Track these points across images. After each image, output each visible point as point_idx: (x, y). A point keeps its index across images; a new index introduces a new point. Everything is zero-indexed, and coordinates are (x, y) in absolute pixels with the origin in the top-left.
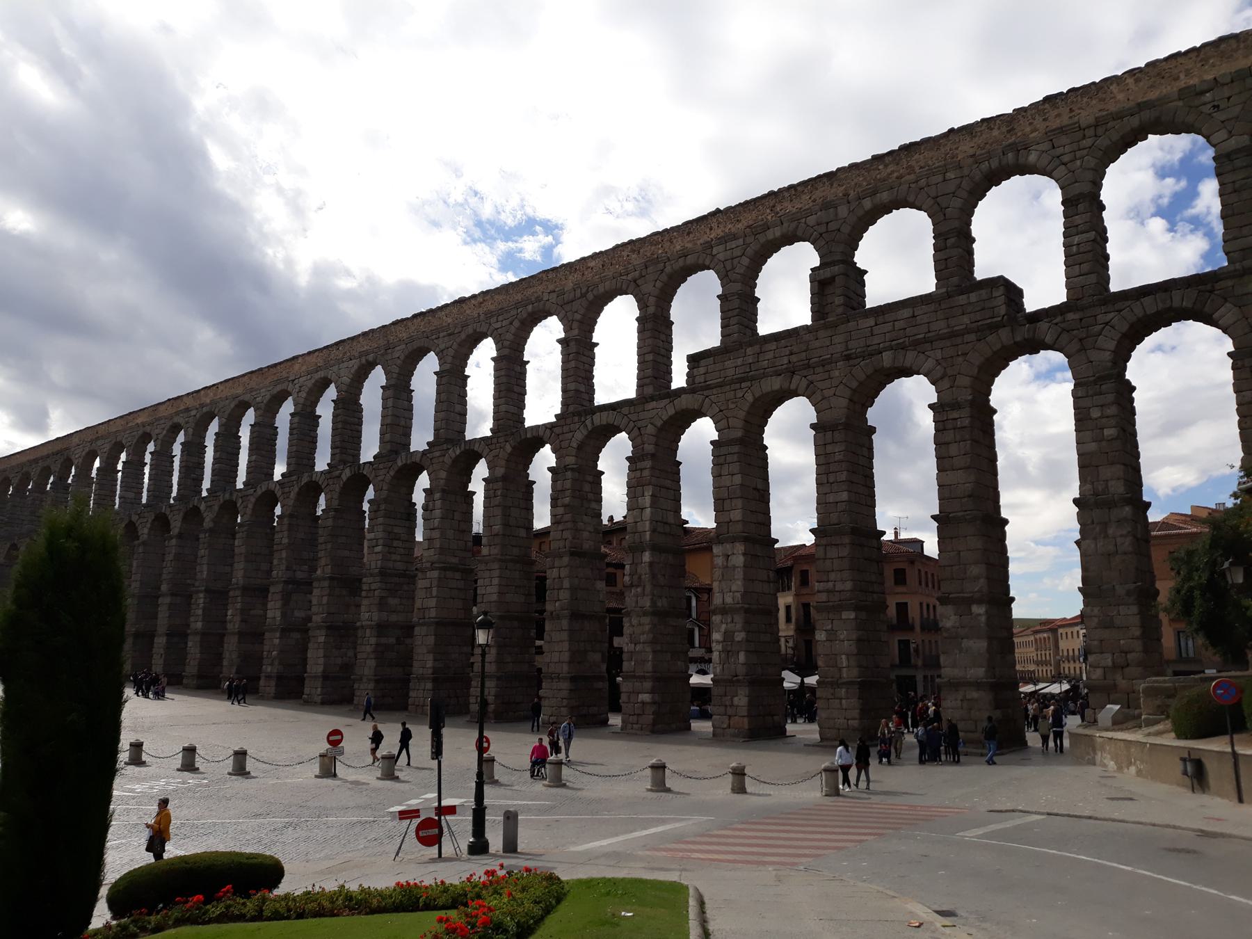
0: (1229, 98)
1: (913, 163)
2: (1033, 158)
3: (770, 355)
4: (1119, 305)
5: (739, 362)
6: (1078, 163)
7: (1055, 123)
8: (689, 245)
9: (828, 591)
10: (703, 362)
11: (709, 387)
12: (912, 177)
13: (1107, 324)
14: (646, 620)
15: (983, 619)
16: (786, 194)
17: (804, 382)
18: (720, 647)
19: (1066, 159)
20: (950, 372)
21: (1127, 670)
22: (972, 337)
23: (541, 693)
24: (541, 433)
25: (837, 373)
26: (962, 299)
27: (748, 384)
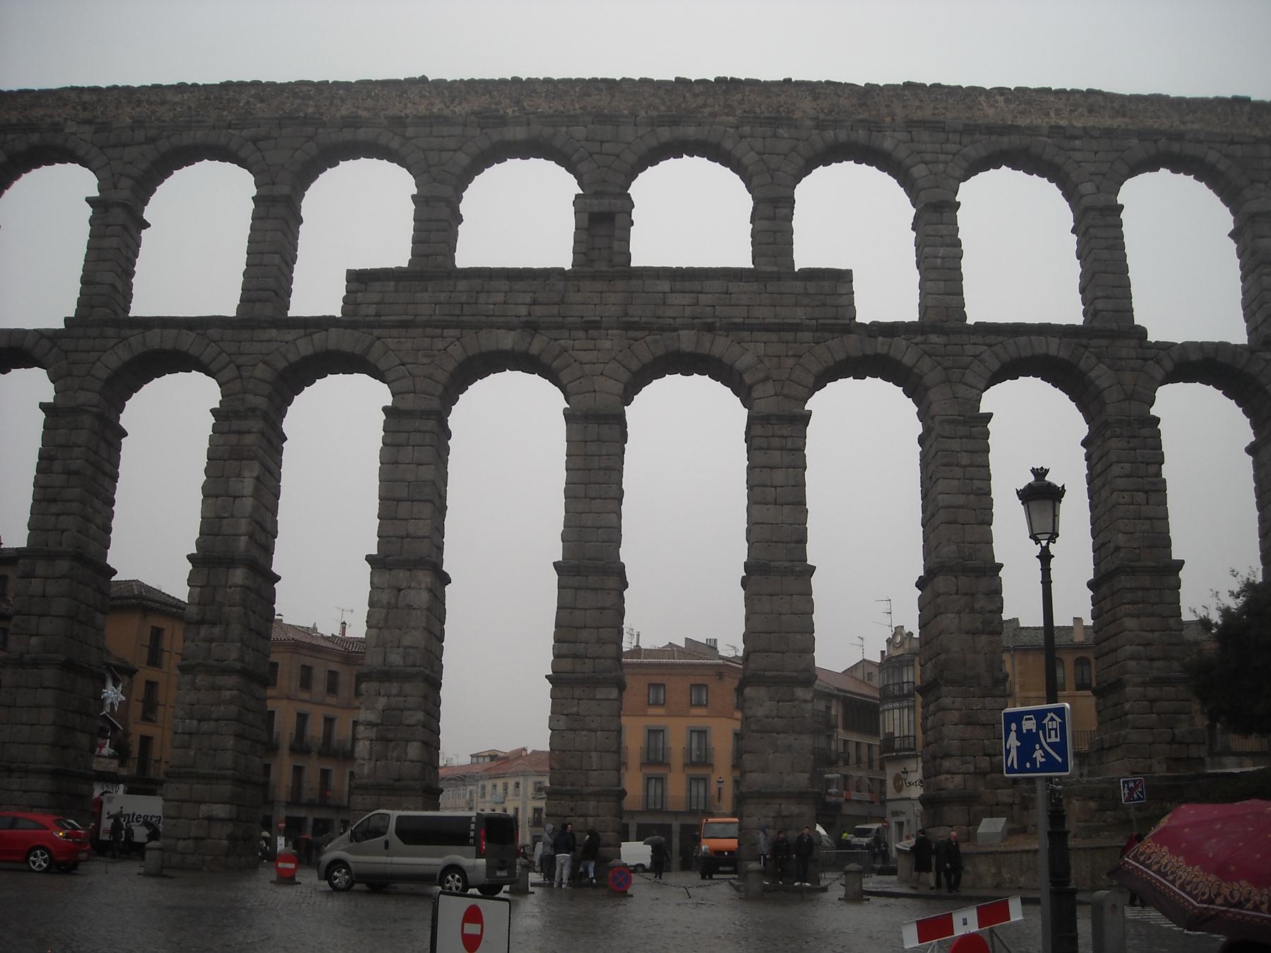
0: (1096, 153)
2: (888, 144)
3: (500, 297)
4: (991, 339)
5: (443, 297)
6: (941, 167)
7: (918, 115)
9: (575, 656)
10: (377, 286)
11: (381, 325)
13: (975, 357)
14: (232, 680)
18: (372, 733)
19: (928, 157)
21: (988, 777)
22: (807, 336)
27: (456, 332)
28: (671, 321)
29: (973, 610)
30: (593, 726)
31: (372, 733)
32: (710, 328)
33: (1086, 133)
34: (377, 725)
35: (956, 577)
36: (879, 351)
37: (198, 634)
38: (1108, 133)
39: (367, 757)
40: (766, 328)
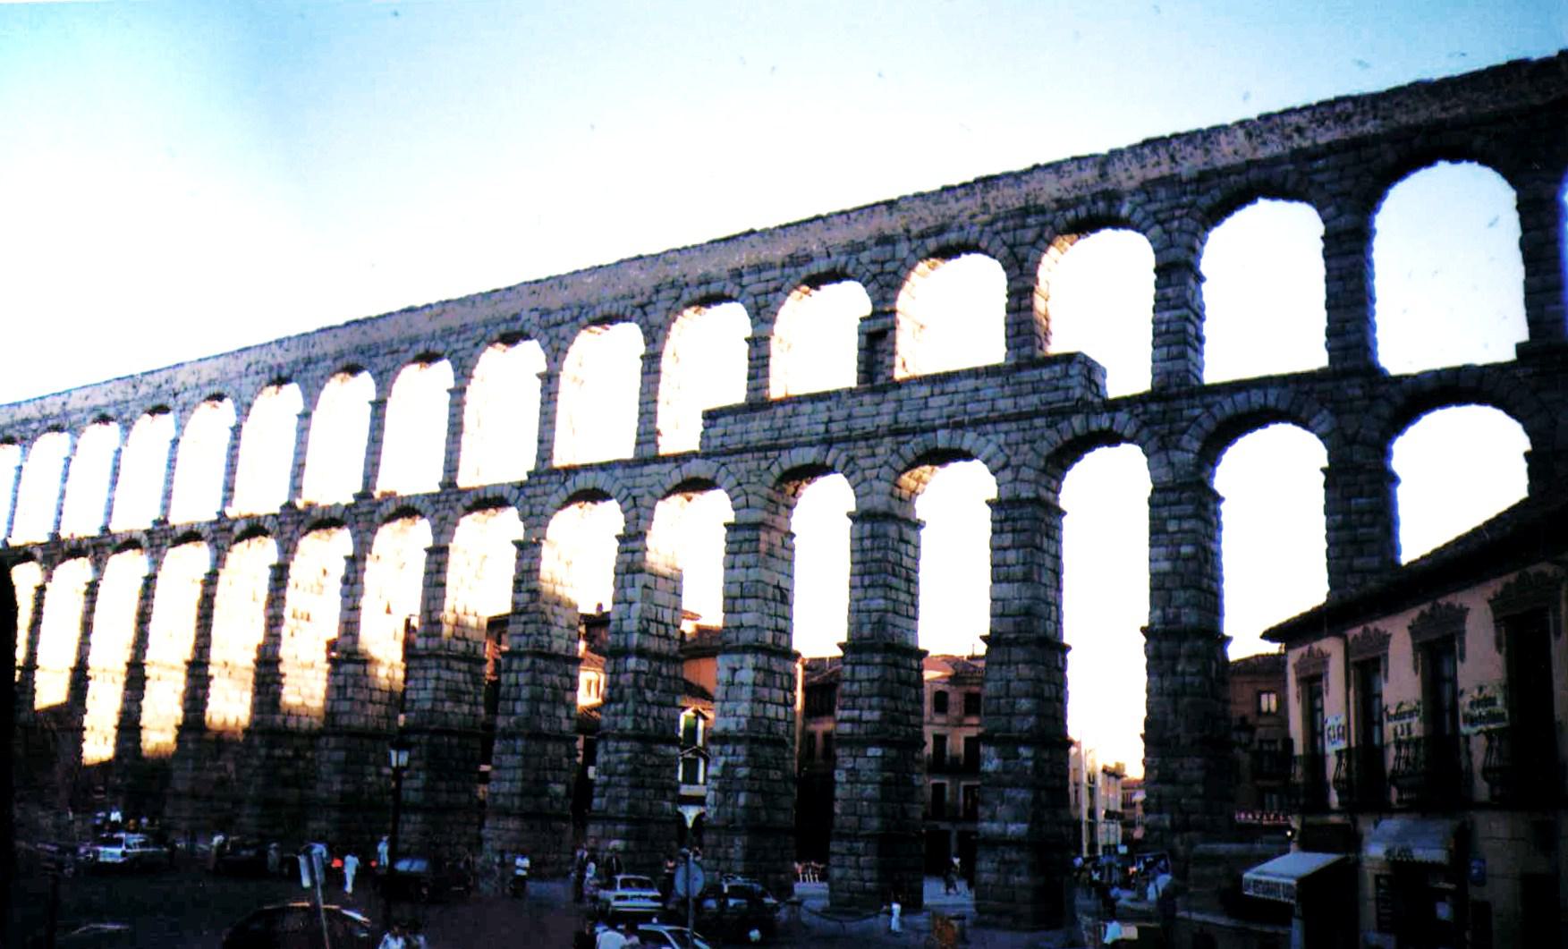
1: (989, 200)
5: (766, 424)
6: (1176, 224)
7: (1153, 174)
8: (714, 271)
10: (721, 421)
12: (986, 218)
14: (624, 746)
15: (1030, 764)
16: (836, 220)
17: (843, 458)
19: (1162, 216)
20: (1014, 461)
22: (1039, 422)
23: (483, 832)
24: (505, 495)
25: (880, 450)
26: (1034, 374)
27: (776, 453)
32: (959, 426)
33: (1331, 148)
38: (1356, 144)
40: (1006, 418)
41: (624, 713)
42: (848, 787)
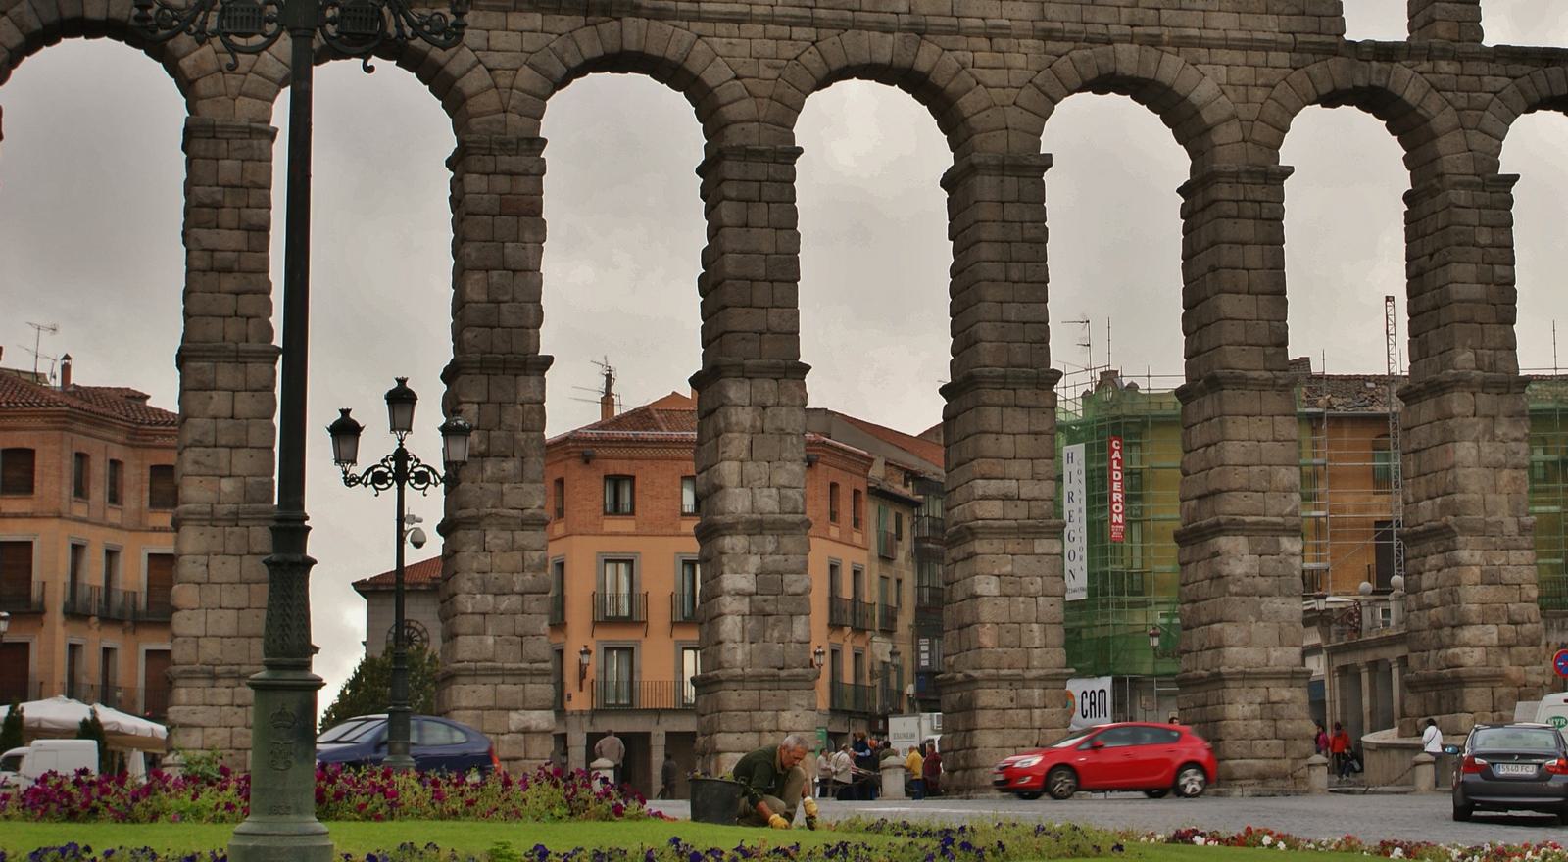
9: (1006, 497)
11: (699, 17)
13: (1495, 93)
18: (744, 605)
21: (1514, 651)
27: (811, 33)
28: (1101, 29)
29: (1493, 438)
30: (1032, 589)
31: (744, 605)
32: (1155, 42)
34: (750, 594)
35: (1474, 394)
36: (1374, 82)
37: (482, 470)
39: (738, 638)
41: (521, 477)
42: (1003, 602)
